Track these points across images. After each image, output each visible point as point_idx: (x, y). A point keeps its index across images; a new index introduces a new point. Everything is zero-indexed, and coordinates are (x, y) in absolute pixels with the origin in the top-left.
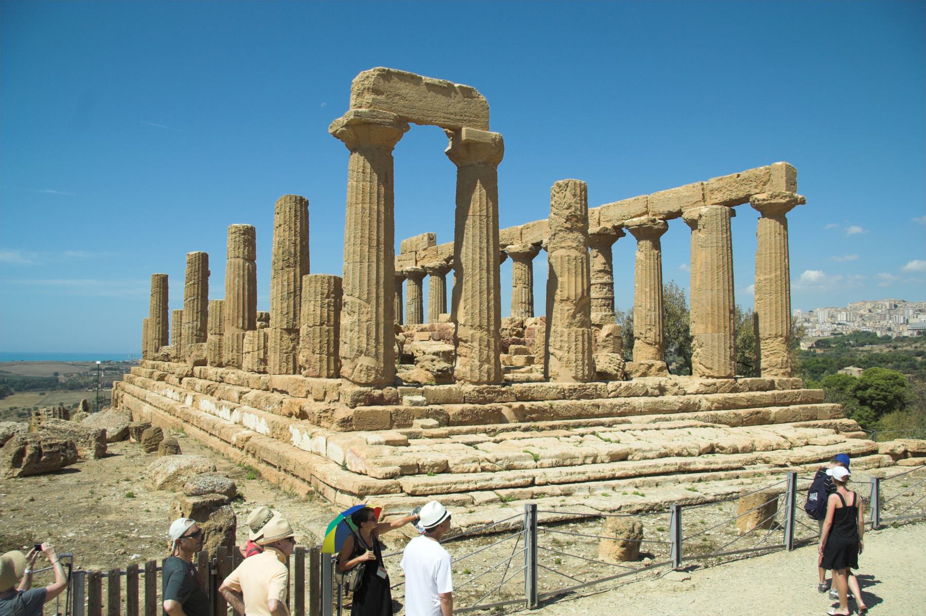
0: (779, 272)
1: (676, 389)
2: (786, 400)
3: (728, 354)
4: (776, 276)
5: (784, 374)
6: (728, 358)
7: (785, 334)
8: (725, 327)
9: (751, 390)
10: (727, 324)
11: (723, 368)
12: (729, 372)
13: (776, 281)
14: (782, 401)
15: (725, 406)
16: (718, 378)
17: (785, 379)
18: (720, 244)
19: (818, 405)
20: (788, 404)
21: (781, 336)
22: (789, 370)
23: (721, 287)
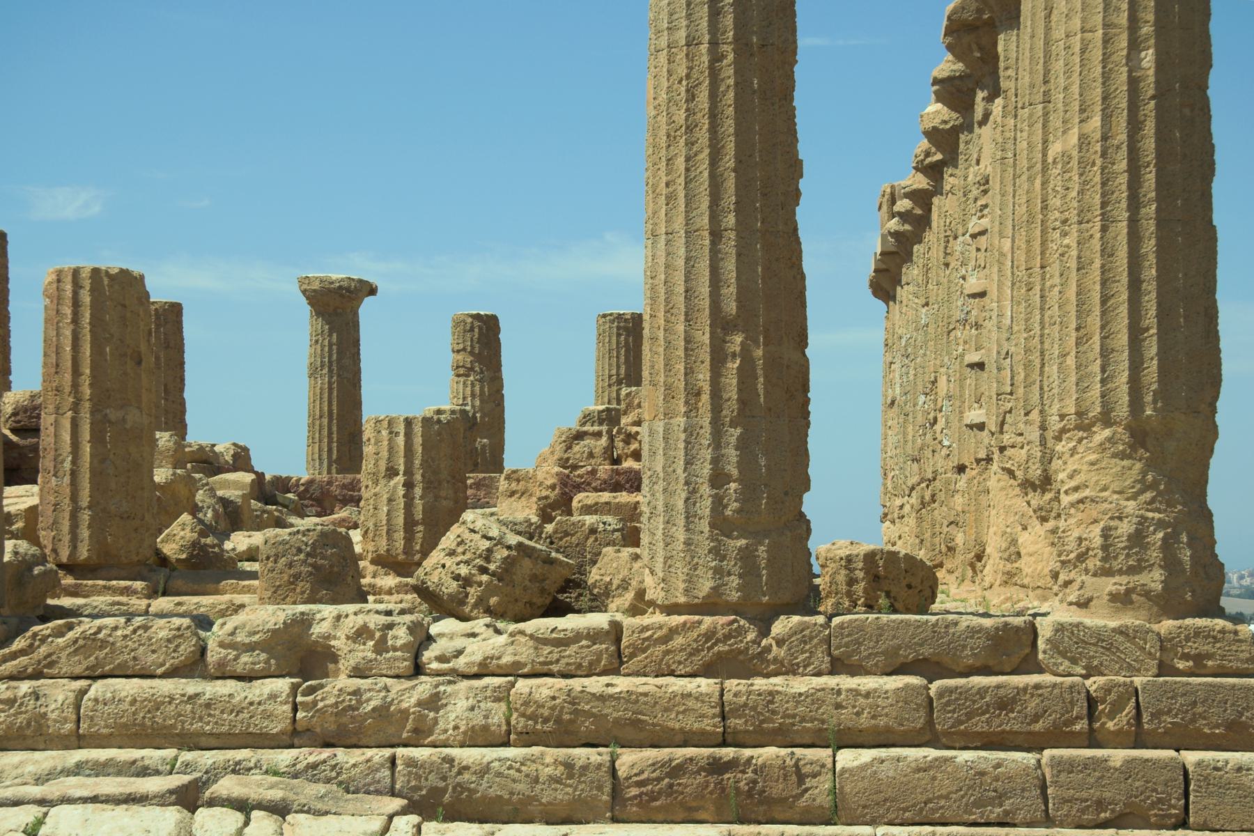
0: (1096, 121)
1: (365, 651)
2: (1012, 723)
3: (705, 507)
4: (1083, 138)
5: (1122, 600)
6: (704, 526)
7: (1122, 410)
8: (693, 393)
9: (837, 666)
10: (703, 377)
11: (681, 570)
12: (705, 586)
13: (1084, 164)
14: (979, 724)
15: (562, 728)
16: (671, 610)
17: (1129, 620)
18: (681, 35)
19: (1191, 757)
20: (1034, 744)
21: (1106, 419)
22: (1154, 579)
23: (679, 223)
